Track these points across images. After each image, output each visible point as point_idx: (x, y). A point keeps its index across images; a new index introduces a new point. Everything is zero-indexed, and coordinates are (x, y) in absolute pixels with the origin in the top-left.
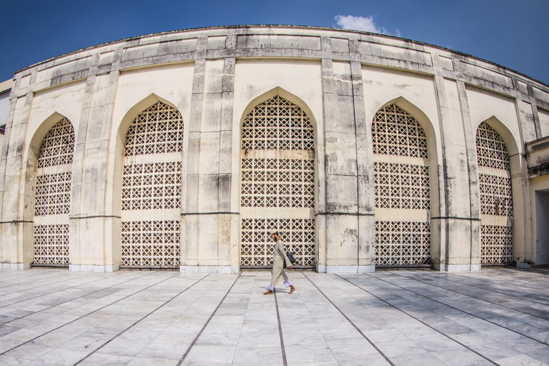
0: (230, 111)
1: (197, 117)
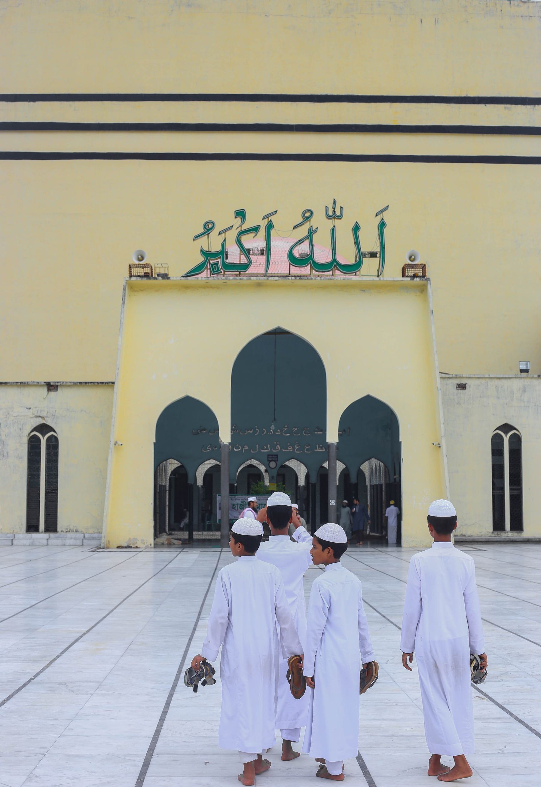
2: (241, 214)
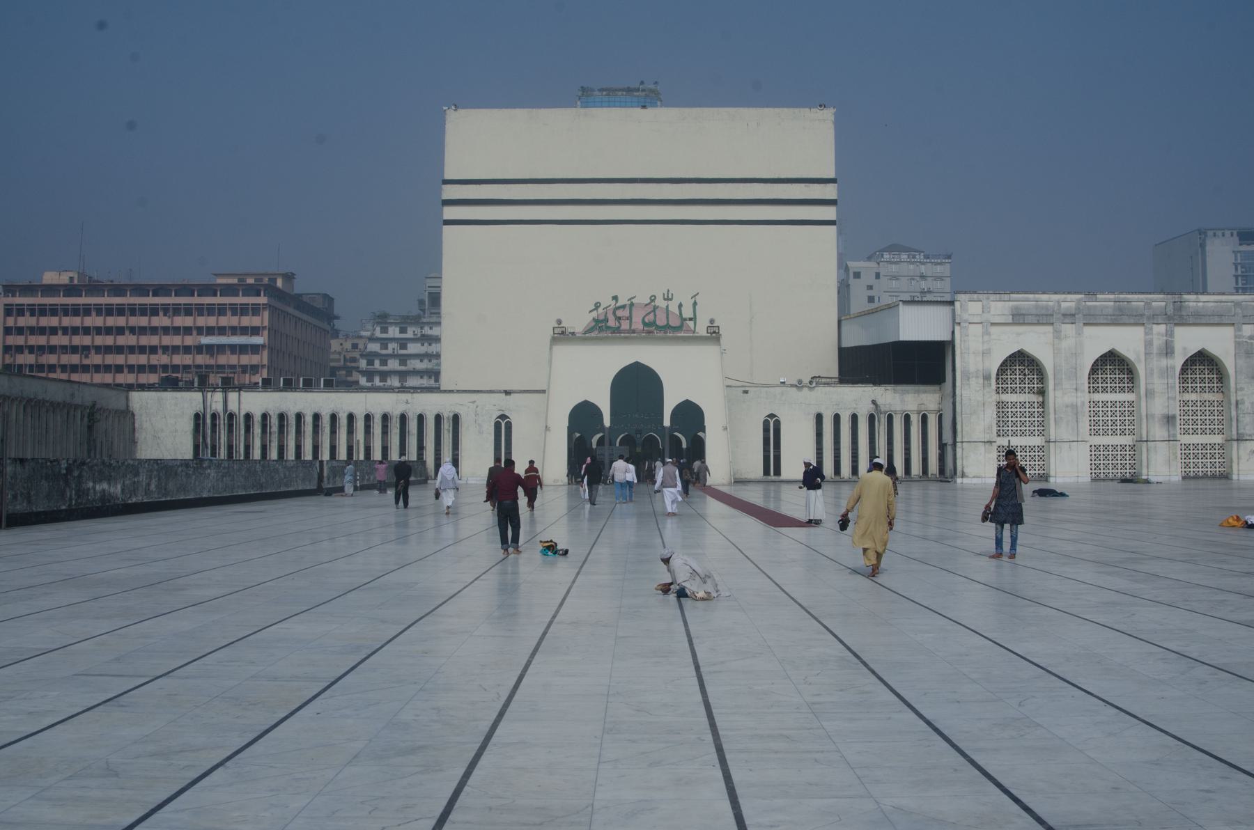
0: (1173, 368)
1: (1150, 373)
2: (615, 298)
